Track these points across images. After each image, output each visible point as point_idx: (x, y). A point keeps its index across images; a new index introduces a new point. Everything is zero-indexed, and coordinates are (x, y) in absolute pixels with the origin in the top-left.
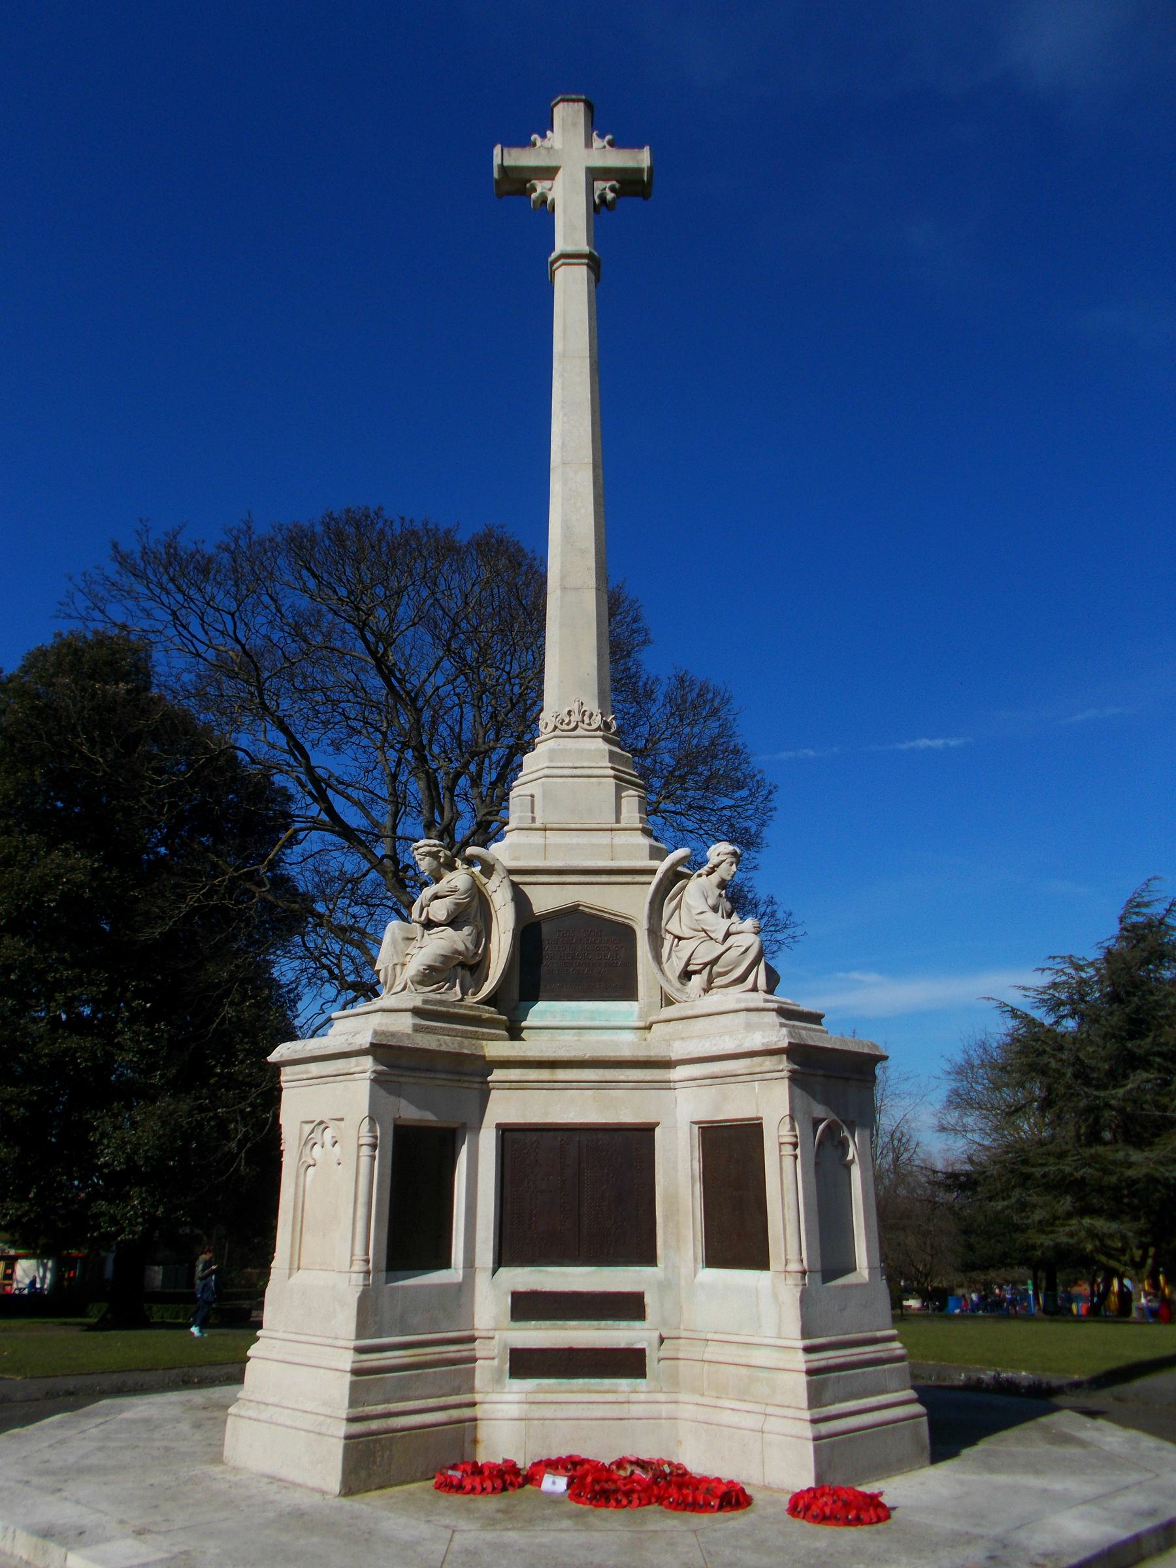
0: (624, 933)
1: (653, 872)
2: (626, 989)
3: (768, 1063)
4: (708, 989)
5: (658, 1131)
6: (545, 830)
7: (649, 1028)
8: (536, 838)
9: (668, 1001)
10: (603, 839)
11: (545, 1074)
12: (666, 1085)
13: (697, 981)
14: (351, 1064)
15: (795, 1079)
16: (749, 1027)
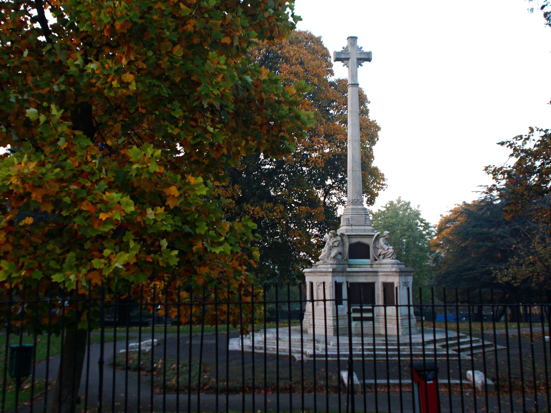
0: (367, 247)
1: (374, 235)
2: (368, 257)
3: (395, 274)
4: (383, 258)
5: (376, 284)
6: (351, 225)
7: (372, 264)
8: (350, 228)
9: (376, 260)
10: (363, 228)
11: (356, 274)
12: (377, 276)
13: (381, 257)
14: (328, 274)
15: (400, 276)
16: (392, 267)
